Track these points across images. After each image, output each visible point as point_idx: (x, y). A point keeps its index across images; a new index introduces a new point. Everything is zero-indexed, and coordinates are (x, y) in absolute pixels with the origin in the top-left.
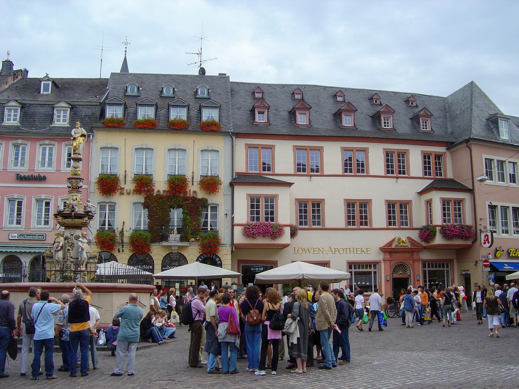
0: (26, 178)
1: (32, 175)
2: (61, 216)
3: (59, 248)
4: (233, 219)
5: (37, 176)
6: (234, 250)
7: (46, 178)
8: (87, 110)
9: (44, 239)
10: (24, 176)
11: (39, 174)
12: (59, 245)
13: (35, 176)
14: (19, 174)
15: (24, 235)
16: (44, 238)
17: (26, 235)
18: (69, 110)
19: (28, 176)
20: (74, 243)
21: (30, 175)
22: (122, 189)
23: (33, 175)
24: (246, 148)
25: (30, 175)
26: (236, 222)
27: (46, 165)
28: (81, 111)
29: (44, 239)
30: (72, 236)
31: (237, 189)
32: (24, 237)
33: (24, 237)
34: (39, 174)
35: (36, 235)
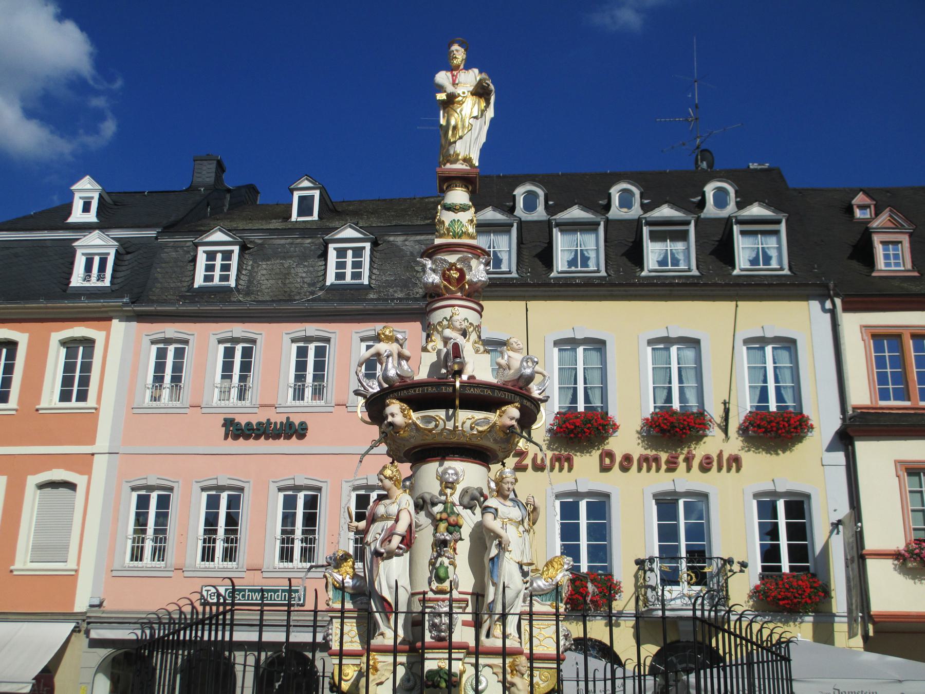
0: (253, 430)
1: (268, 420)
2: (401, 400)
3: (396, 540)
4: (859, 537)
5: (282, 423)
6: (871, 633)
7: (307, 429)
8: (417, 247)
9: (302, 602)
10: (248, 424)
11: (288, 418)
12: (393, 528)
13: (276, 423)
14: (233, 420)
15: (244, 590)
16: (300, 600)
17: (250, 590)
18: (368, 245)
19: (259, 424)
20: (461, 522)
21: (264, 421)
22: (522, 454)
23: (273, 421)
24: (866, 338)
25: (264, 421)
26: (870, 544)
27: (308, 392)
28: (403, 250)
29: (302, 602)
30: (449, 491)
31: (862, 447)
32: (244, 596)
33: (244, 596)
34: (288, 418)
35: (278, 591)
